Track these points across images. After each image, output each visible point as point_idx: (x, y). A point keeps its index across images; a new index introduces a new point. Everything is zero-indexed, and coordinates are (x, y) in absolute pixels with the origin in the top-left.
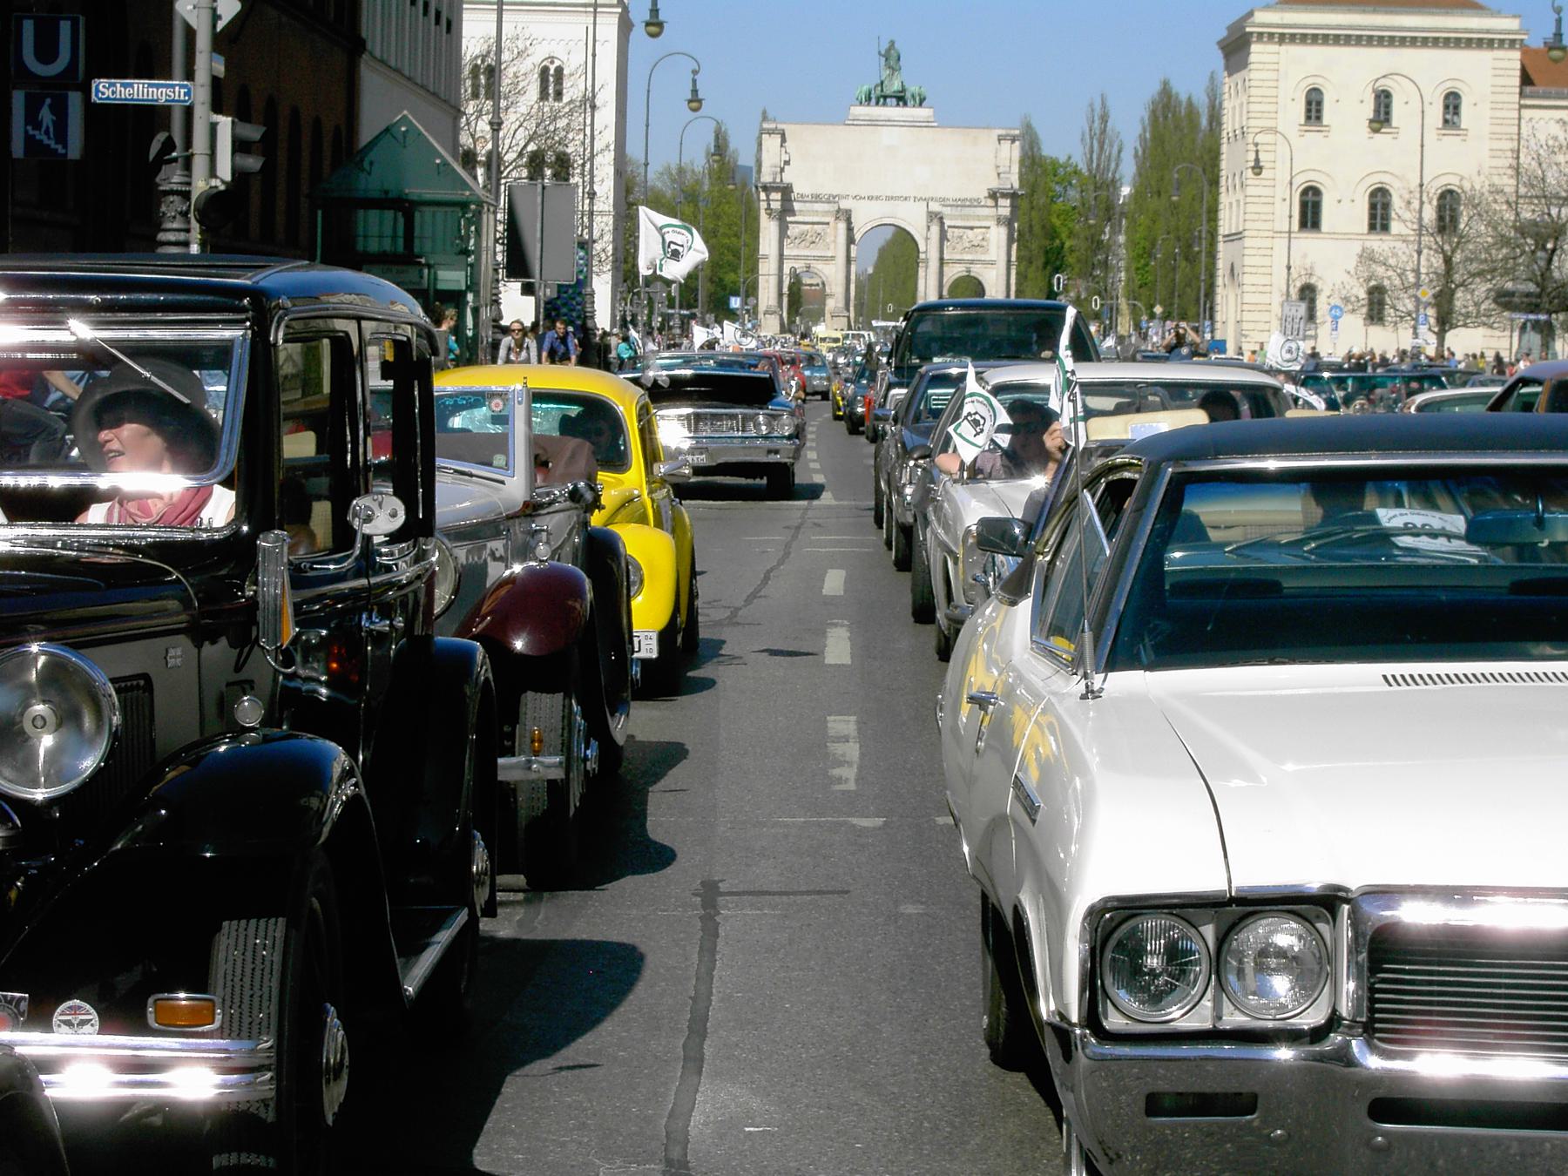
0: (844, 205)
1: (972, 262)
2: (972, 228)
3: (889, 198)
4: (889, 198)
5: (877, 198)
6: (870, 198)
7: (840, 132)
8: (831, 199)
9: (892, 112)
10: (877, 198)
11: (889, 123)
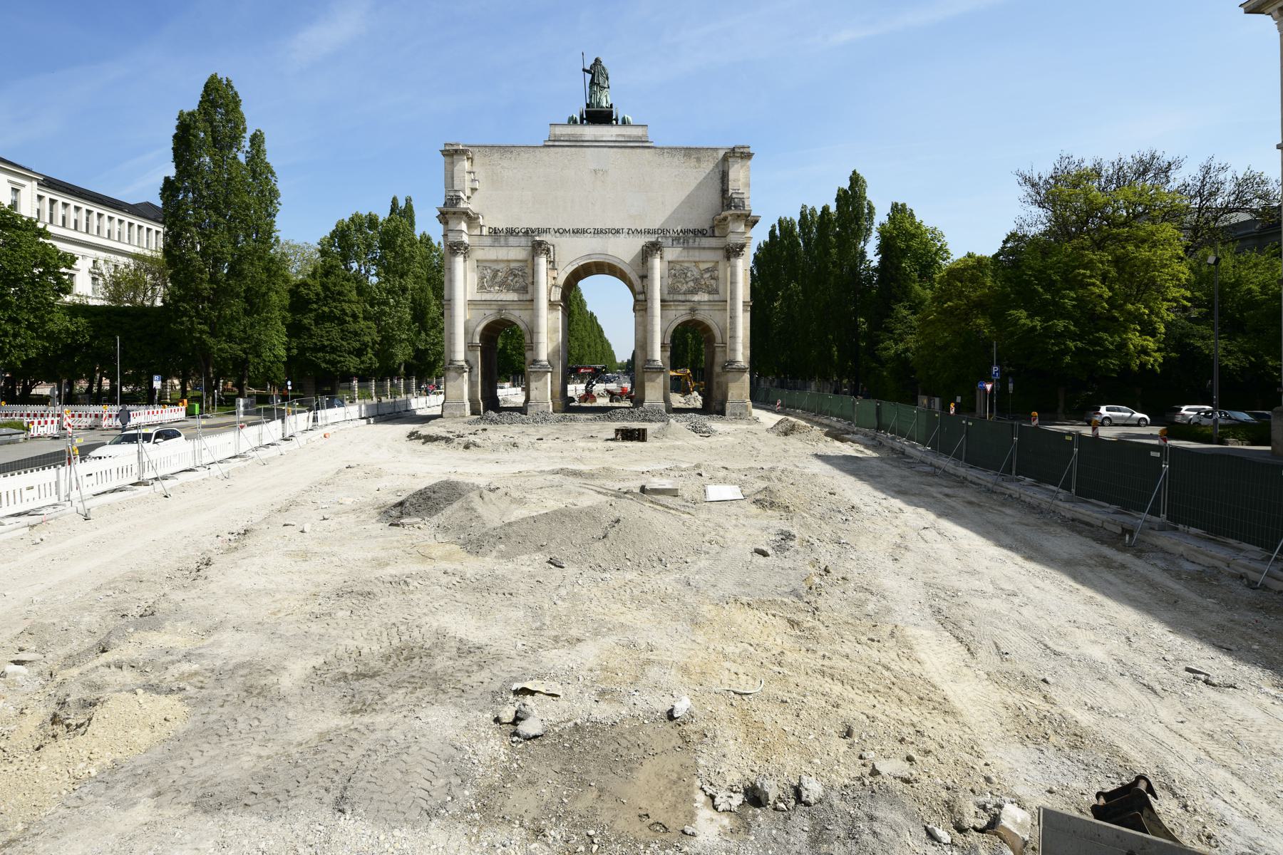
3: (598, 232)
4: (598, 232)
5: (584, 232)
6: (576, 232)
8: (528, 233)
10: (584, 232)
11: (597, 144)
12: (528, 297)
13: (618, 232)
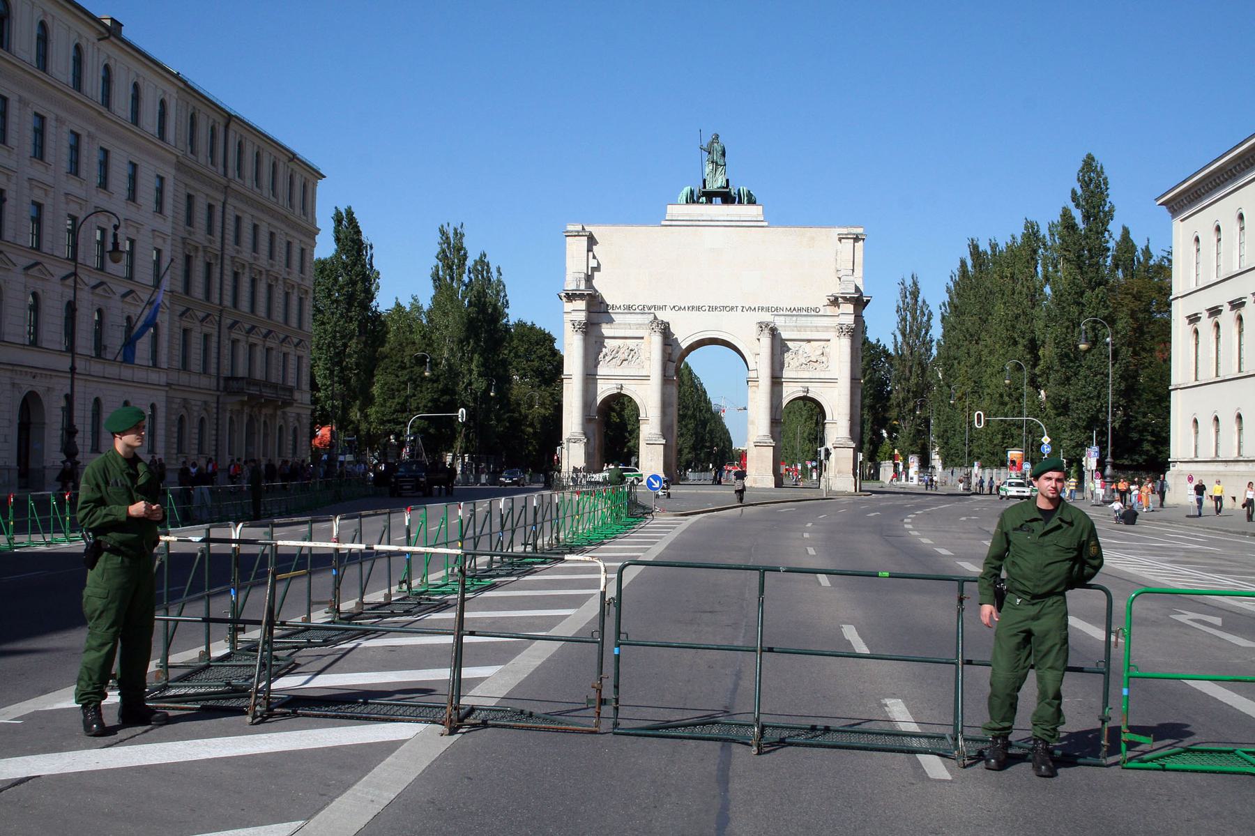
0: (662, 316)
1: (811, 380)
2: (809, 341)
3: (711, 309)
4: (711, 309)
5: (699, 309)
8: (644, 310)
9: (718, 210)
10: (699, 309)
11: (711, 223)
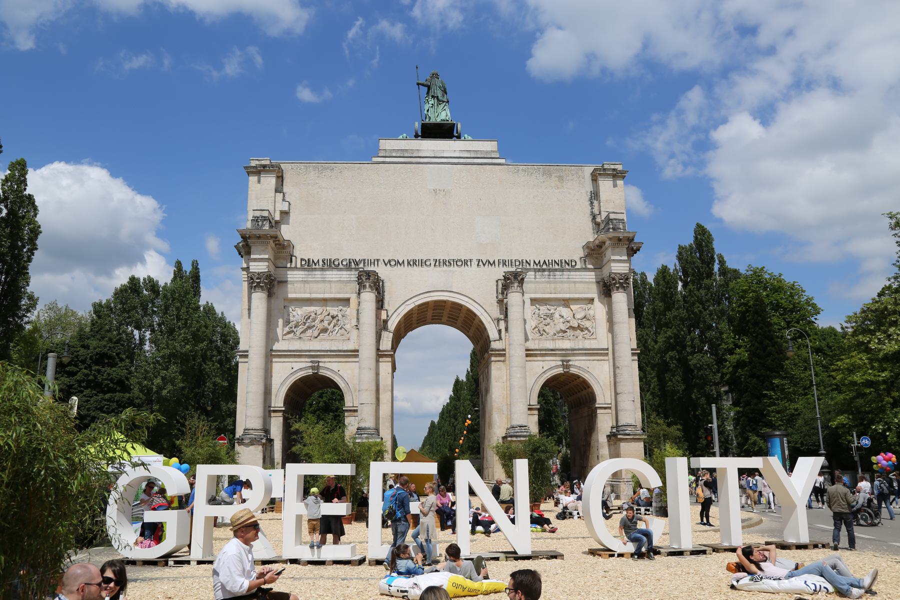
1: (573, 352)
2: (566, 303)
3: (438, 263)
4: (438, 263)
5: (423, 263)
6: (413, 263)
7: (367, 171)
8: (351, 265)
10: (423, 263)
12: (351, 346)
13: (465, 263)
